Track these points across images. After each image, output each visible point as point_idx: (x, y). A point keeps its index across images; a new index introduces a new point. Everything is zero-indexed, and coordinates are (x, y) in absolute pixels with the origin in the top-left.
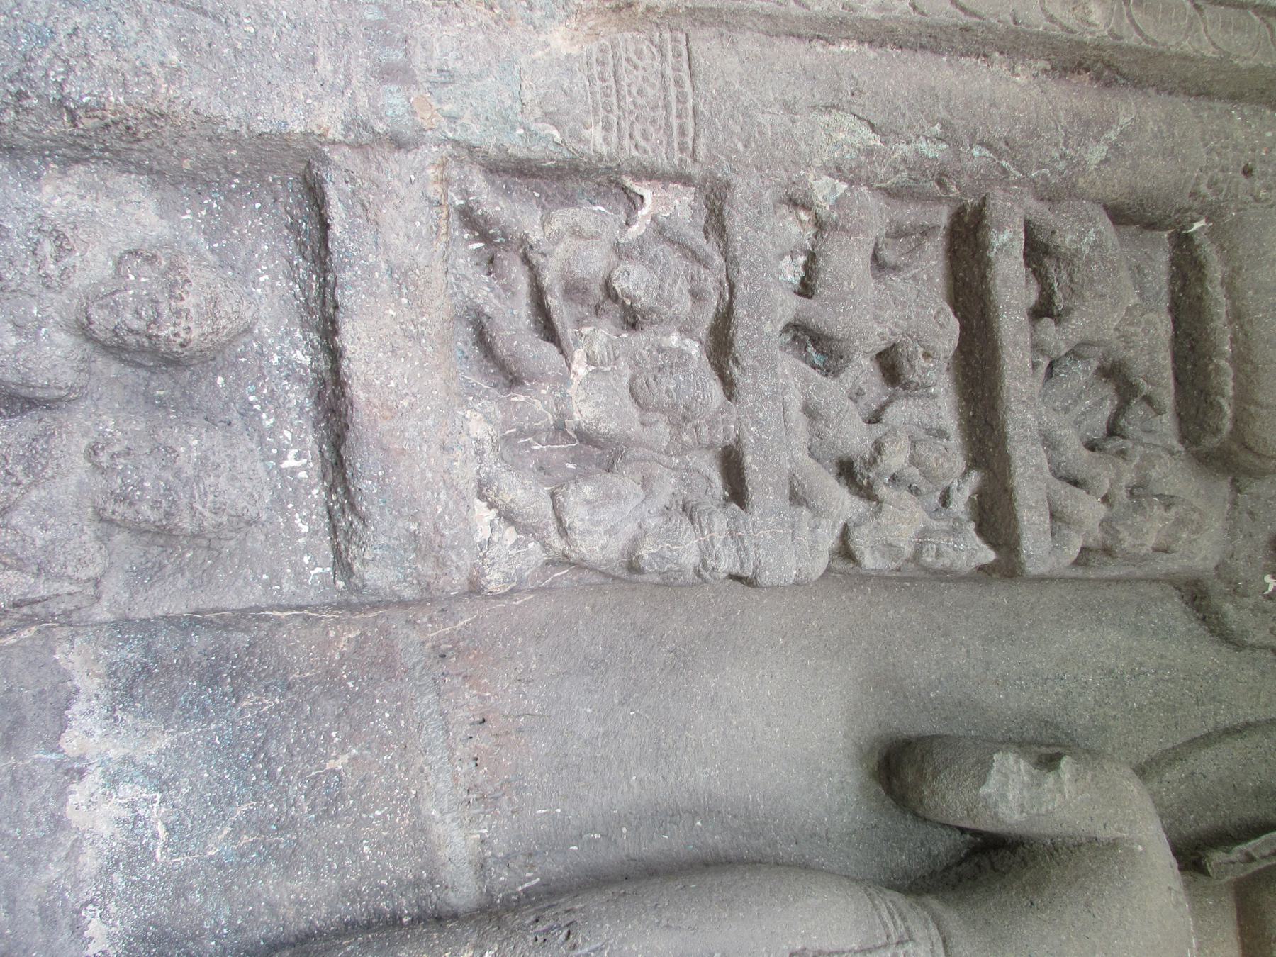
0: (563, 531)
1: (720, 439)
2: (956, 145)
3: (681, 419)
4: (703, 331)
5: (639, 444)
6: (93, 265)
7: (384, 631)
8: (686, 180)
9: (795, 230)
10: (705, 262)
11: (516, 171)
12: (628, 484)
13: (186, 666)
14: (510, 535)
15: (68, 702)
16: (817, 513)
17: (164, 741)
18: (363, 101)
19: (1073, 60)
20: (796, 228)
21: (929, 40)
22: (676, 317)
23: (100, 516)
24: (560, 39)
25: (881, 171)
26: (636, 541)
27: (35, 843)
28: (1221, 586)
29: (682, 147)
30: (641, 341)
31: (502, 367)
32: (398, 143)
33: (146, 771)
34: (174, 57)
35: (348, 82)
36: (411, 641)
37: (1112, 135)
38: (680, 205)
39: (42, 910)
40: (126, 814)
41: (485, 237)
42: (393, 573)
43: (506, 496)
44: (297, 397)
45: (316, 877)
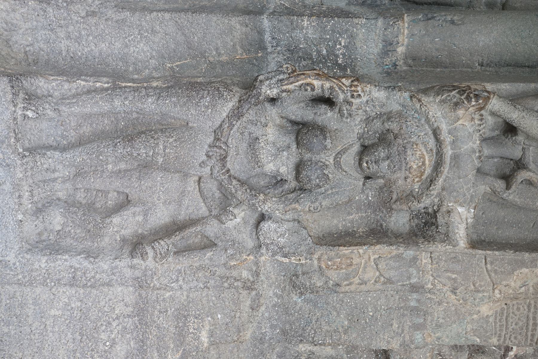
18: (407, 338)
34: (346, 323)
35: (403, 331)
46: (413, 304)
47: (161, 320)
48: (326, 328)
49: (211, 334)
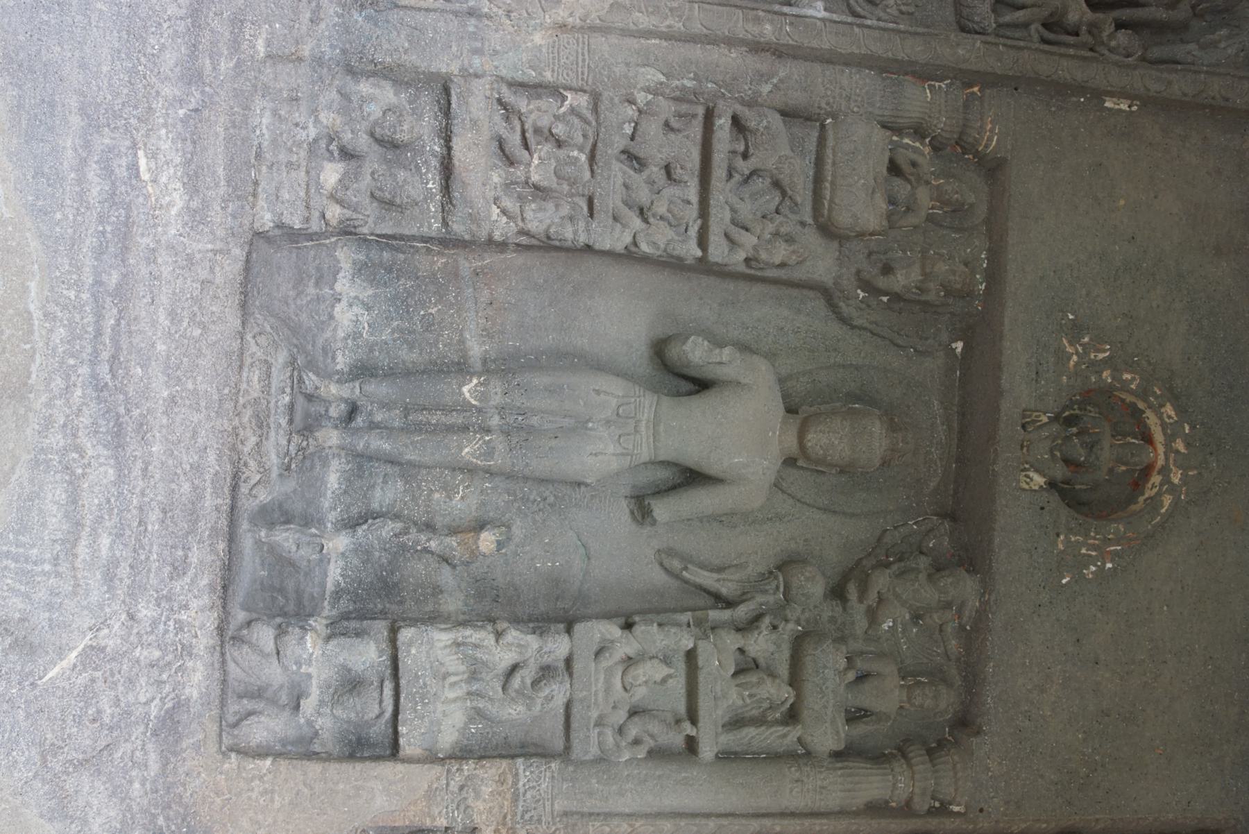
0: (523, 220)
2: (700, 82)
3: (572, 184)
4: (587, 150)
6: (374, 110)
7: (456, 261)
8: (585, 91)
9: (631, 113)
10: (589, 123)
11: (519, 86)
12: (550, 206)
13: (381, 264)
14: (504, 219)
15: (338, 272)
16: (624, 226)
17: (370, 292)
18: (466, 62)
20: (631, 111)
21: (692, 39)
23: (372, 195)
26: (549, 227)
27: (323, 322)
28: (838, 294)
30: (562, 153)
31: (508, 158)
32: (477, 76)
33: (363, 303)
36: (467, 264)
37: (775, 81)
38: (583, 101)
39: (323, 349)
41: (505, 109)
42: (462, 228)
43: (503, 204)
44: (434, 162)
46: (471, 29)
47: (215, 24)
48: (386, 46)
49: (268, 44)
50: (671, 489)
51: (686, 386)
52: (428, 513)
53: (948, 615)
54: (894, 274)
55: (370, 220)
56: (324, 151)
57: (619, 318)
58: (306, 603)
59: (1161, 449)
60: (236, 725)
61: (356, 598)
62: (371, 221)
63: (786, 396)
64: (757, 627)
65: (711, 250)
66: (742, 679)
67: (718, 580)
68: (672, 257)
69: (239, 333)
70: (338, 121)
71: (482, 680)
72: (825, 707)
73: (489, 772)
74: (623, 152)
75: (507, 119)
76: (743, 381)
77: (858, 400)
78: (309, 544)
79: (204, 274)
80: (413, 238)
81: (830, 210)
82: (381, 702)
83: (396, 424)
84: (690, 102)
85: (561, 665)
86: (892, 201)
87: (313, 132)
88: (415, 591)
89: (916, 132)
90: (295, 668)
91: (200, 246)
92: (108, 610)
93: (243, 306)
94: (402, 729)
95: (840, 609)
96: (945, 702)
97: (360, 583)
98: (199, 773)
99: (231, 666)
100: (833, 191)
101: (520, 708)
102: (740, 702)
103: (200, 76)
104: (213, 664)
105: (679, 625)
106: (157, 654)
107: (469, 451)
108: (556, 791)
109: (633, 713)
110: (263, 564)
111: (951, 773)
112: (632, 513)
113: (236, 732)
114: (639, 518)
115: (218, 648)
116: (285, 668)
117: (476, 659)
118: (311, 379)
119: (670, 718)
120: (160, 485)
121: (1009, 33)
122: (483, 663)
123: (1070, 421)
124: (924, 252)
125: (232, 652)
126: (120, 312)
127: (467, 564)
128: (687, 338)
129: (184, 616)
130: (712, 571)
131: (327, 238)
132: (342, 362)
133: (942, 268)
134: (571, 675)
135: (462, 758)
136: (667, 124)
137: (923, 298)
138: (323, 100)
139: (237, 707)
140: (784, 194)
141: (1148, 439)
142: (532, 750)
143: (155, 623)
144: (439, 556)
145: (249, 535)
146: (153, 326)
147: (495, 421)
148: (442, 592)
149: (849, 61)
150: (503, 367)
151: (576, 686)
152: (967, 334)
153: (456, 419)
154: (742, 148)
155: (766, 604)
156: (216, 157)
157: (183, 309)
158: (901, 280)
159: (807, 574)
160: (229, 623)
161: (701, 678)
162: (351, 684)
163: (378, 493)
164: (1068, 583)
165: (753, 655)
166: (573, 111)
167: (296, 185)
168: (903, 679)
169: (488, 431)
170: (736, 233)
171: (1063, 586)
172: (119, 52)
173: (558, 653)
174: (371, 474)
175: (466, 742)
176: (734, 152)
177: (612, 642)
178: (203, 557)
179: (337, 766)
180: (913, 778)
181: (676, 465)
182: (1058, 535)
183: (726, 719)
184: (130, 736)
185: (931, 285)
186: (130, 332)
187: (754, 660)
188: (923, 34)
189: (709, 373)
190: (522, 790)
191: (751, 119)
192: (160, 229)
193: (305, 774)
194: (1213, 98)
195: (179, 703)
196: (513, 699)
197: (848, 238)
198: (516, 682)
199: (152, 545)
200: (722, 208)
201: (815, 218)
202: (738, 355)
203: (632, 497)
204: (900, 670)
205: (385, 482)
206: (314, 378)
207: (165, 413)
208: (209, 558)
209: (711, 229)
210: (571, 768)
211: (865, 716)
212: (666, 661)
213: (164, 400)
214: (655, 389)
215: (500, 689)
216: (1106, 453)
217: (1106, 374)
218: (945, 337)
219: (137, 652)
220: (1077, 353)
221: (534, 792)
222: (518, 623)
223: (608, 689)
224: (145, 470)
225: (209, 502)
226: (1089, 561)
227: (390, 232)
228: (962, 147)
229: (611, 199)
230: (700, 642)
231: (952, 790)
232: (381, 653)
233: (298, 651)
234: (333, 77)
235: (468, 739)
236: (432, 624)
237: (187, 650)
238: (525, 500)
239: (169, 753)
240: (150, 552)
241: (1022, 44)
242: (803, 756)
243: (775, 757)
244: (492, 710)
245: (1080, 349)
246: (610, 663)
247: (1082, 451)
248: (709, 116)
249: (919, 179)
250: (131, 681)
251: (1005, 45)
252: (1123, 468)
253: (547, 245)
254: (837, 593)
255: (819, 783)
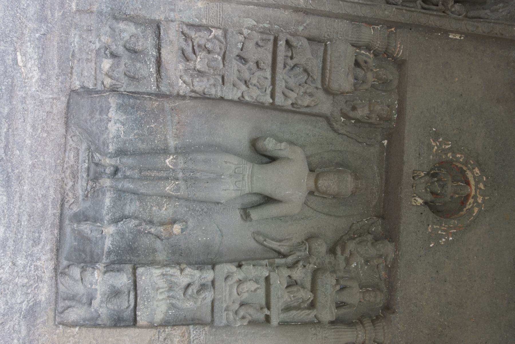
0: (193, 86)
1: (221, 73)
2: (272, 25)
4: (222, 55)
5: (208, 73)
6: (126, 36)
7: (163, 103)
8: (221, 29)
9: (241, 38)
10: (222, 43)
11: (191, 26)
12: (205, 79)
14: (185, 85)
15: (110, 108)
17: (124, 117)
18: (167, 15)
19: (297, 10)
20: (241, 38)
22: (216, 53)
23: (125, 74)
24: (200, 5)
25: (257, 29)
26: (204, 89)
27: (103, 131)
28: (332, 119)
29: (219, 23)
30: (210, 56)
31: (186, 58)
32: (172, 21)
33: (121, 122)
34: (140, 7)
36: (168, 105)
37: (305, 25)
40: (117, 129)
41: (185, 36)
42: (166, 89)
43: (184, 79)
44: (153, 60)
45: (147, 145)
48: (131, 7)
49: (77, 5)
50: (259, 205)
51: (266, 160)
52: (150, 216)
53: (381, 261)
54: (357, 110)
55: (124, 85)
56: (103, 54)
57: (236, 130)
58: (95, 257)
59: (473, 188)
60: (62, 312)
61: (117, 254)
62: (124, 86)
63: (309, 164)
64: (297, 266)
65: (276, 99)
66: (290, 289)
67: (280, 246)
68: (259, 102)
69: (65, 135)
70: (110, 41)
71: (175, 290)
72: (326, 301)
73: (177, 333)
74: (238, 56)
75: (186, 40)
76: (290, 157)
77: (341, 166)
78: (96, 230)
79: (48, 109)
80: (144, 93)
81: (329, 82)
82: (129, 301)
83: (136, 176)
84: (267, 34)
85: (210, 284)
86: (356, 78)
87: (98, 45)
88: (144, 251)
89: (367, 48)
90: (89, 286)
91: (46, 96)
92: (3, 261)
93: (66, 123)
94: (138, 313)
95: (333, 258)
96: (380, 299)
97: (119, 247)
98: (45, 335)
99: (60, 286)
100: (330, 73)
101: (191, 303)
102: (289, 300)
103: (46, 19)
104: (52, 285)
105: (262, 265)
106: (26, 281)
107: (169, 188)
108: (207, 340)
109: (242, 305)
110: (75, 239)
111: (382, 331)
112: (241, 216)
113: (62, 316)
114: (245, 218)
115: (54, 278)
116: (85, 286)
117: (171, 281)
118: (97, 156)
119: (258, 307)
120: (28, 204)
121: (407, 5)
122: (175, 283)
123: (434, 175)
124: (370, 101)
125: (61, 279)
126: (9, 125)
127: (168, 239)
128: (266, 138)
129: (38, 263)
130: (277, 241)
131: (104, 93)
132: (111, 148)
133: (378, 108)
134: (214, 288)
135: (165, 326)
136: (257, 44)
137: (370, 121)
138: (102, 31)
139: (63, 304)
140: (309, 75)
141: (468, 183)
142: (197, 322)
143: (25, 267)
144: (155, 235)
145: (69, 226)
146: (24, 132)
147: (180, 175)
148: (156, 251)
149: (337, 16)
150: (184, 151)
151: (216, 293)
152: (389, 137)
153: (163, 174)
154: (290, 54)
155: (301, 256)
156: (54, 55)
157: (38, 124)
158: (360, 113)
159: (319, 243)
160: (59, 266)
161: (272, 289)
162: (115, 293)
163: (128, 207)
164: (433, 246)
165: (295, 278)
166: (215, 37)
167: (90, 69)
168: (361, 289)
169: (177, 179)
170: (287, 92)
171: (431, 248)
172: (8, 7)
173: (208, 278)
174: (124, 199)
175: (167, 319)
176: (287, 56)
177: (233, 273)
178: (47, 236)
179: (109, 330)
180: (365, 333)
181: (261, 194)
182: (428, 225)
183: (283, 307)
184: (13, 318)
185: (373, 115)
186: (14, 135)
187: (295, 281)
188: (370, 5)
189: (275, 154)
190: (192, 340)
191: (294, 42)
192: (27, 88)
193: (94, 334)
194: (496, 34)
195: (36, 303)
196: (188, 299)
197: (337, 95)
198: (190, 291)
199: (24, 231)
200: (281, 81)
201: (322, 86)
202: (288, 146)
203: (241, 209)
204: (359, 285)
205: (131, 202)
206: (99, 155)
207: (30, 171)
208: (50, 237)
209: (276, 90)
210: (214, 330)
211: (344, 305)
212: (257, 281)
213: (30, 166)
214: (251, 160)
215: (182, 295)
216: (449, 189)
217: (449, 155)
218: (379, 138)
219: (16, 280)
220: (437, 145)
221: (197, 341)
222: (191, 265)
223: (230, 294)
224: (21, 197)
225: (50, 212)
226: (442, 236)
227: (133, 90)
228: (387, 55)
229: (232, 77)
230: (271, 273)
231: (383, 338)
232: (129, 279)
233: (91, 278)
234: (107, 20)
235: (168, 317)
236: (152, 266)
237: (40, 279)
238: (194, 210)
239: (31, 324)
240: (23, 234)
241: (413, 9)
242: (317, 323)
243: (305, 324)
244: (179, 304)
245: (438, 144)
246: (232, 282)
247: (439, 189)
248: (276, 41)
249: (368, 69)
250: (13, 293)
251: (406, 10)
252: (457, 196)
253: (203, 97)
254: (332, 251)
255: (324, 335)
